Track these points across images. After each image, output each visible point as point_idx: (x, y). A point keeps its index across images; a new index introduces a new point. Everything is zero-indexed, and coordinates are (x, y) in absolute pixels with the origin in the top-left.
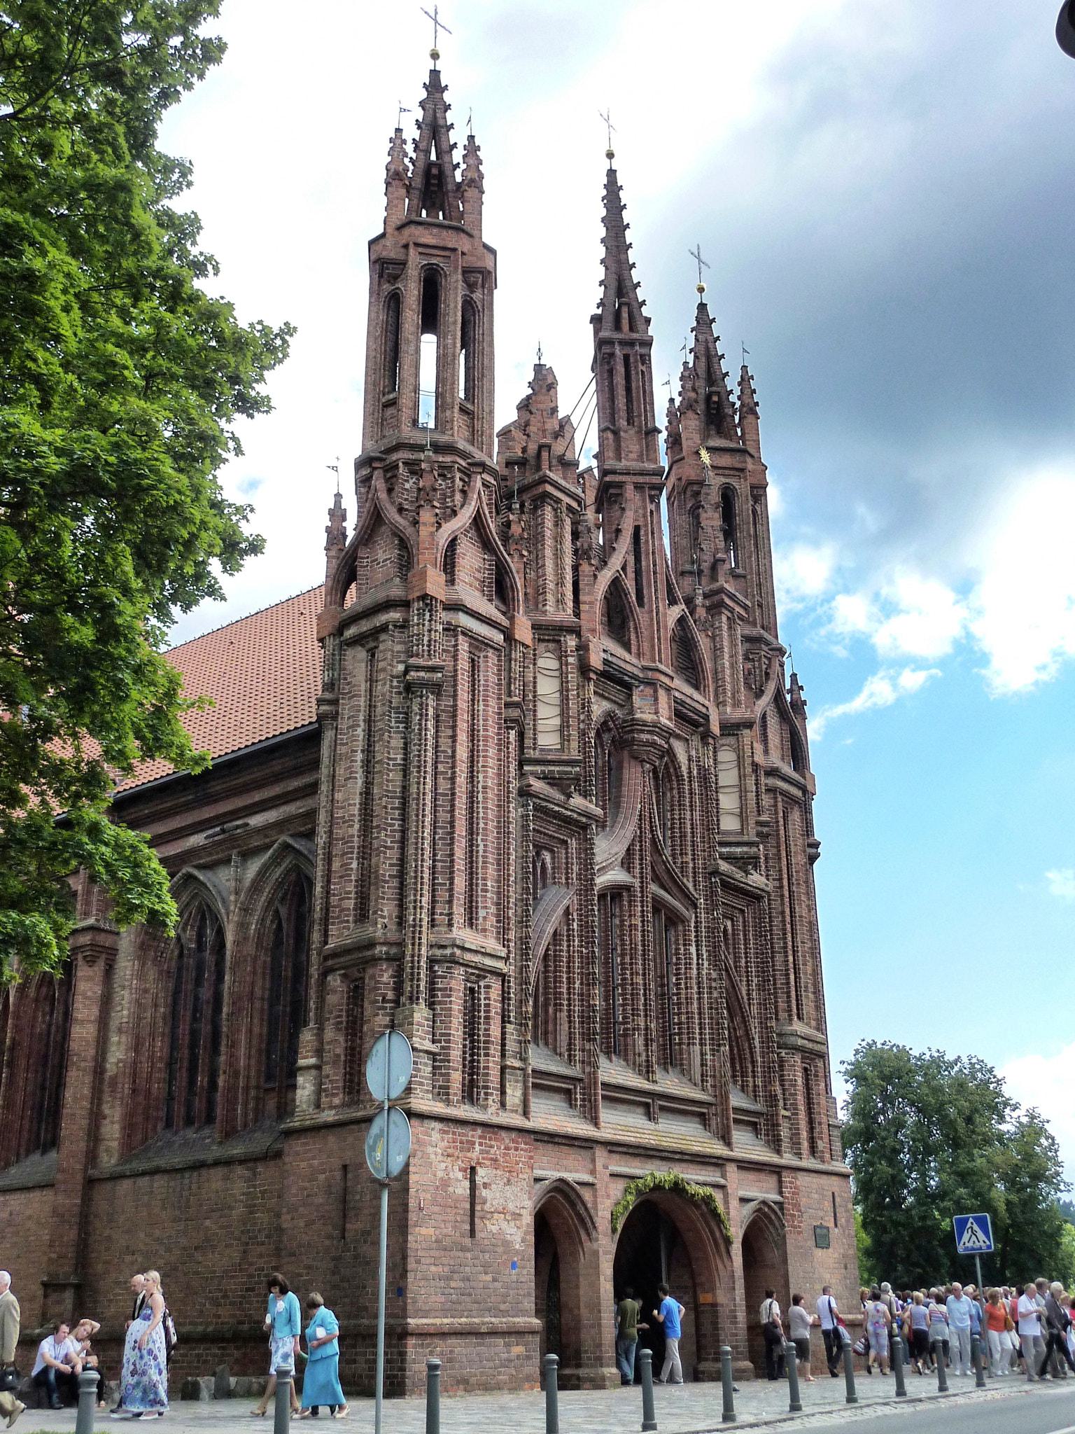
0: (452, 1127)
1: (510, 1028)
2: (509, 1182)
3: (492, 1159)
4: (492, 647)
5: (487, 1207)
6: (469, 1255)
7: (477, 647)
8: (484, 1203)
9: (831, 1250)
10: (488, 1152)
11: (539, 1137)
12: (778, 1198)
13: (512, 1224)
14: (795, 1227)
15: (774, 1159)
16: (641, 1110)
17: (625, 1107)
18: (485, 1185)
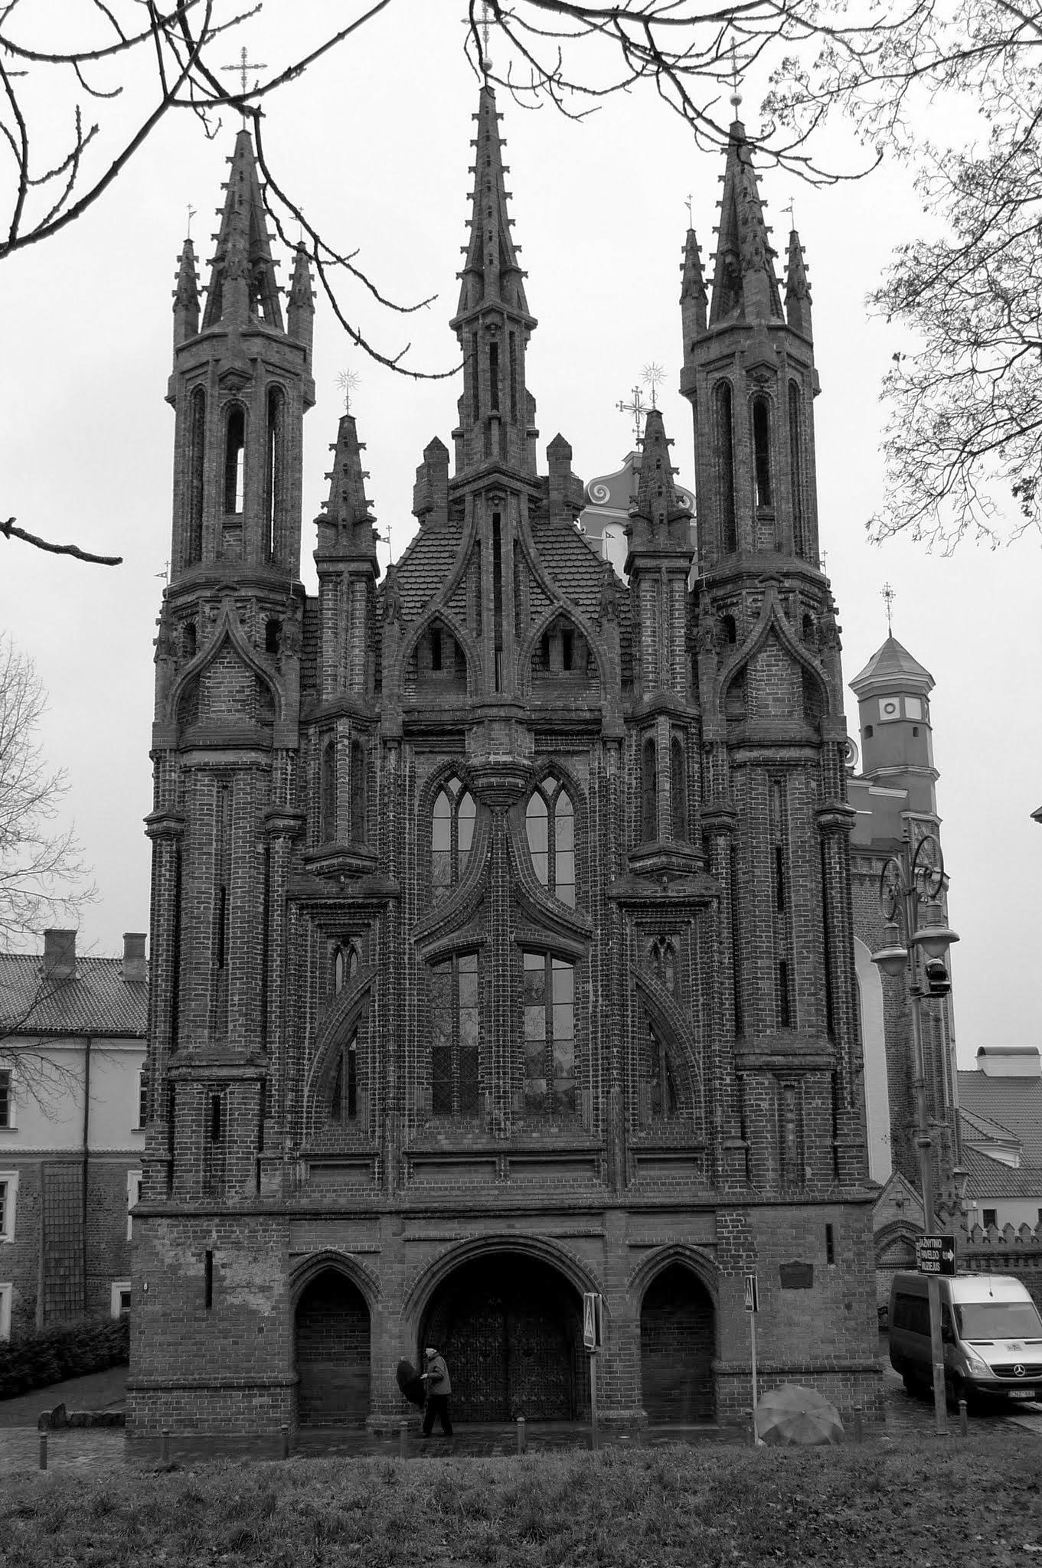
0: (183, 1221)
1: (269, 1123)
2: (255, 1259)
3: (233, 1243)
4: (240, 769)
5: (227, 1283)
6: (204, 1324)
7: (225, 775)
8: (224, 1278)
10: (229, 1237)
11: (292, 1217)
12: (711, 1239)
13: (261, 1295)
15: (706, 1196)
16: (489, 1168)
18: (224, 1266)
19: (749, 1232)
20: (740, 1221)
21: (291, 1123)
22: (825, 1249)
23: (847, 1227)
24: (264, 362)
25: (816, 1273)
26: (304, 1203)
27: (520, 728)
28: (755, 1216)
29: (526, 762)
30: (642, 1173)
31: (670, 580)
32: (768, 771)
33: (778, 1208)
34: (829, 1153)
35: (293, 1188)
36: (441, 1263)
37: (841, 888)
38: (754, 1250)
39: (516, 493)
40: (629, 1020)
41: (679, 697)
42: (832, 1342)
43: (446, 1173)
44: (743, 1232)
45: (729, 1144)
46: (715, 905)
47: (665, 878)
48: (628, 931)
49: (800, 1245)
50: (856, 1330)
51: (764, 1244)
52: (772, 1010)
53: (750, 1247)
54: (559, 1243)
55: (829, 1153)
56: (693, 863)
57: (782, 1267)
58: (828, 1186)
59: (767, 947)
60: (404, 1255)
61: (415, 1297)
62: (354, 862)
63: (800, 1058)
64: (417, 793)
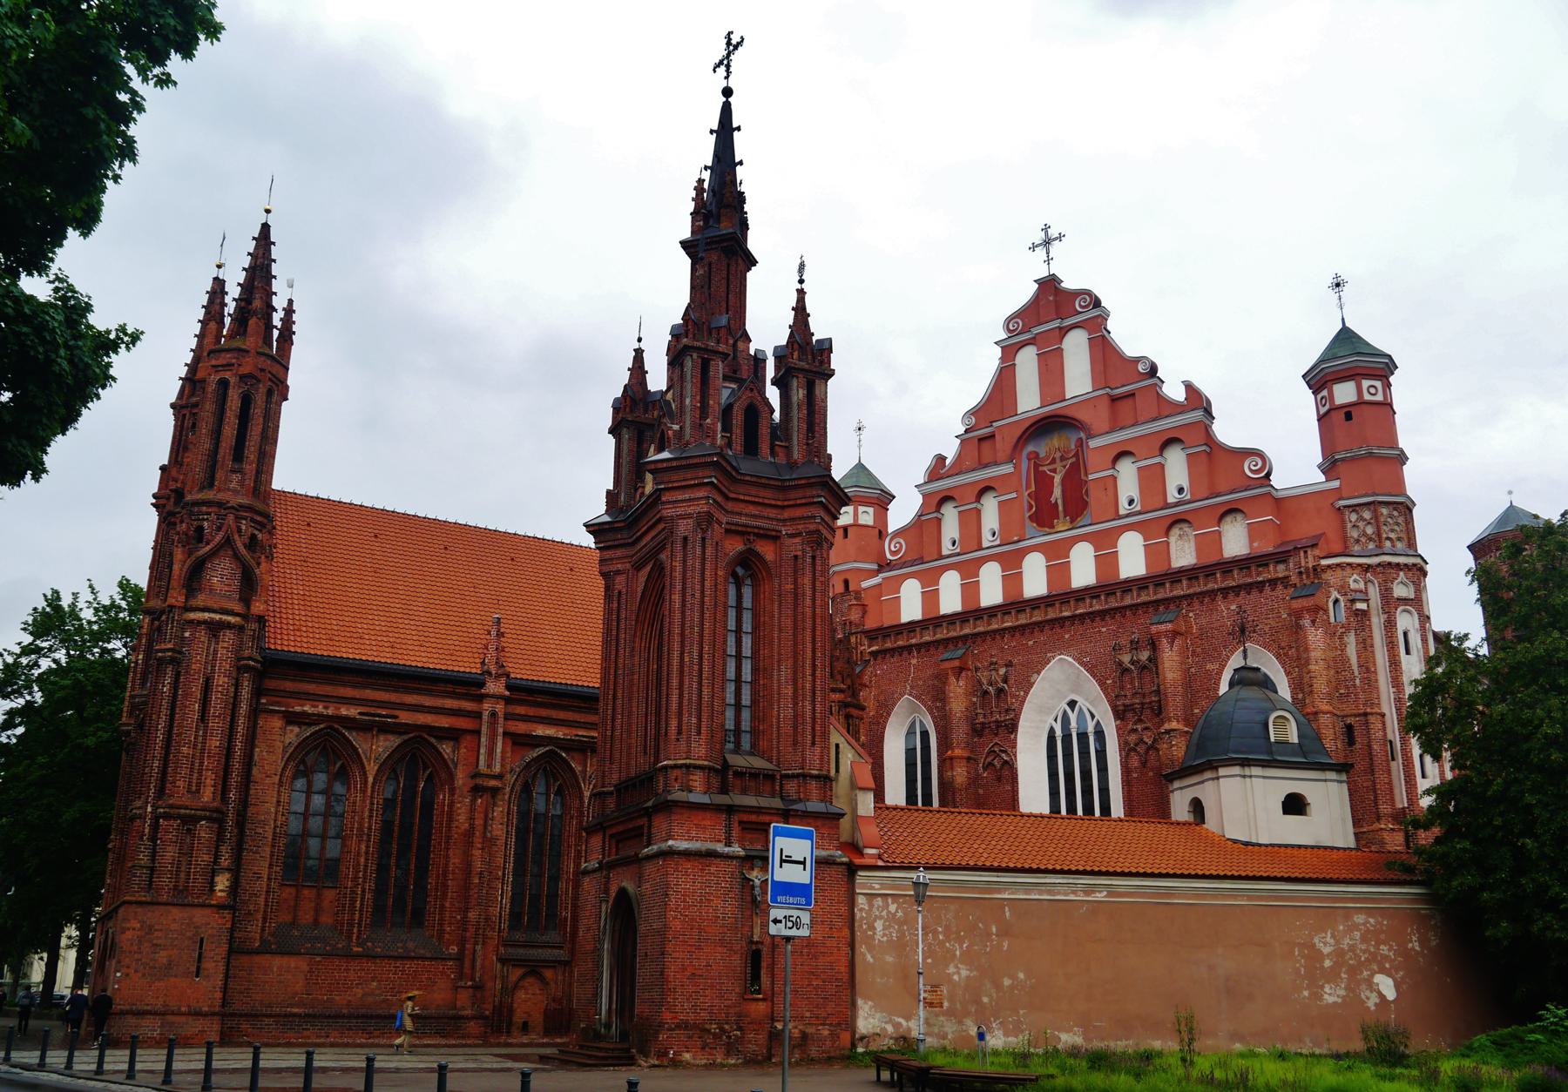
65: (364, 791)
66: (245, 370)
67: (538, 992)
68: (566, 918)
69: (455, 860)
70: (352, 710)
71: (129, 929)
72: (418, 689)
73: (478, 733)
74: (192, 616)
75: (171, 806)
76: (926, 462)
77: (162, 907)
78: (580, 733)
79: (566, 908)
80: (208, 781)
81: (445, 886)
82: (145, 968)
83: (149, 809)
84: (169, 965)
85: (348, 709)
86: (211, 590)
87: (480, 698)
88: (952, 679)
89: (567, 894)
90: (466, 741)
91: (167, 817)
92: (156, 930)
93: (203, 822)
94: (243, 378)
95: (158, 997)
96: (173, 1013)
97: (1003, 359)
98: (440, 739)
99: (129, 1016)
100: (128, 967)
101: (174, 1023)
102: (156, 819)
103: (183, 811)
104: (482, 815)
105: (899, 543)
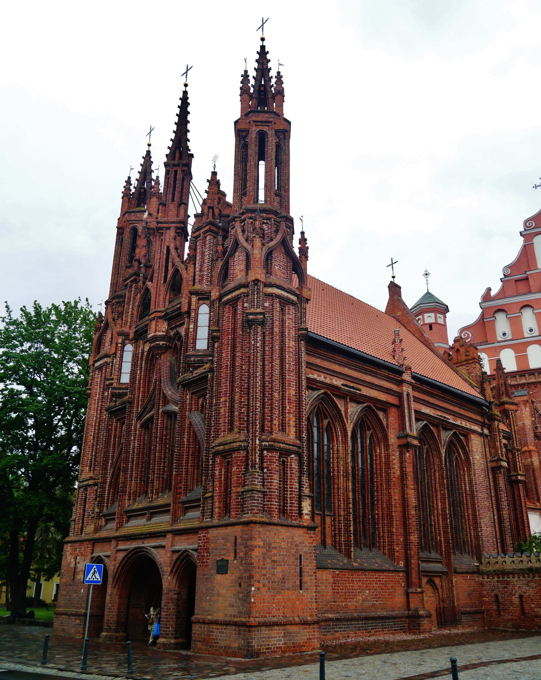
9: (227, 576)
12: (196, 546)
14: (203, 562)
17: (139, 518)
19: (208, 542)
20: (205, 536)
21: (98, 501)
22: (233, 551)
23: (242, 538)
24: (128, 221)
25: (229, 565)
26: (97, 536)
27: (160, 321)
28: (212, 533)
29: (161, 333)
30: (187, 514)
31: (206, 237)
32: (231, 305)
33: (219, 528)
34: (240, 496)
35: (97, 529)
36: (124, 562)
37: (254, 352)
38: (208, 552)
39: (168, 228)
40: (185, 440)
41: (204, 287)
42: (233, 606)
43: (137, 519)
44: (205, 542)
45: (207, 495)
46: (209, 376)
47: (191, 369)
48: (188, 397)
49: (224, 549)
50: (242, 599)
51: (212, 549)
52: (226, 423)
53: (207, 550)
54: (153, 550)
55: (240, 496)
56: (206, 358)
57: (217, 561)
58: (237, 514)
59: (225, 391)
60: (116, 557)
61: (117, 577)
62: (117, 391)
63: (228, 445)
64: (144, 358)
65: (345, 442)
66: (277, 127)
67: (432, 595)
68: (440, 541)
69: (396, 497)
70: (338, 382)
71: (256, 547)
72: (372, 372)
73: (400, 407)
74: (270, 290)
75: (274, 441)
76: (483, 291)
77: (275, 527)
78: (439, 414)
79: (440, 535)
80: (291, 422)
81: (391, 517)
82: (269, 582)
83: (258, 442)
84: (283, 580)
85: (336, 381)
86: (276, 275)
87: (400, 382)
88: (523, 407)
89: (439, 524)
90: (393, 413)
91: (271, 449)
92: (273, 548)
93: (293, 456)
94: (277, 131)
95: (279, 609)
96: (291, 624)
97: (525, 241)
98: (379, 409)
99: (263, 628)
100: (259, 582)
101: (291, 633)
102: (262, 451)
103: (281, 445)
104: (411, 465)
105: (468, 335)
